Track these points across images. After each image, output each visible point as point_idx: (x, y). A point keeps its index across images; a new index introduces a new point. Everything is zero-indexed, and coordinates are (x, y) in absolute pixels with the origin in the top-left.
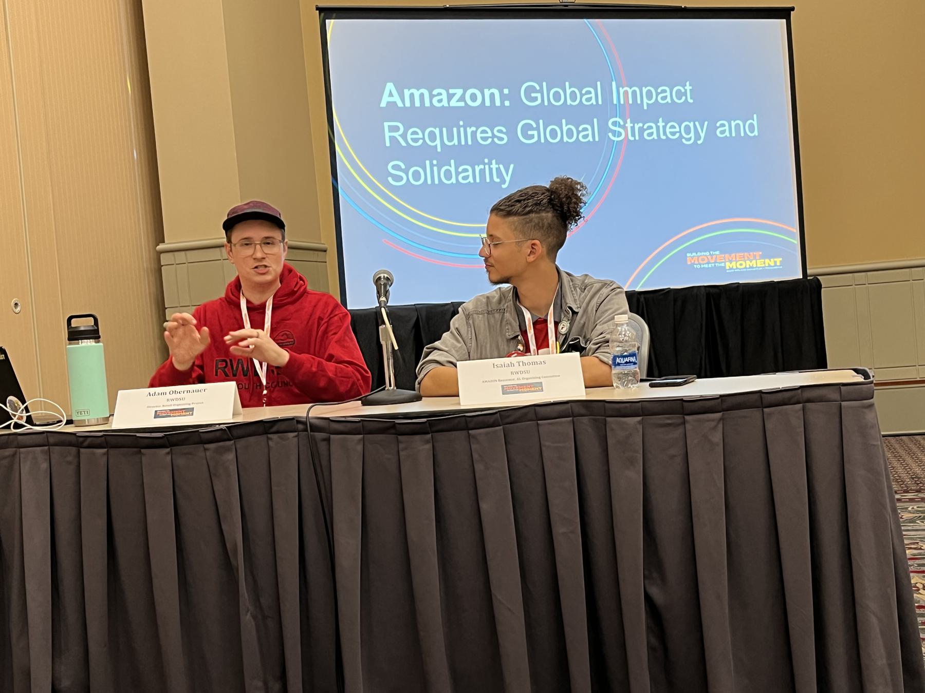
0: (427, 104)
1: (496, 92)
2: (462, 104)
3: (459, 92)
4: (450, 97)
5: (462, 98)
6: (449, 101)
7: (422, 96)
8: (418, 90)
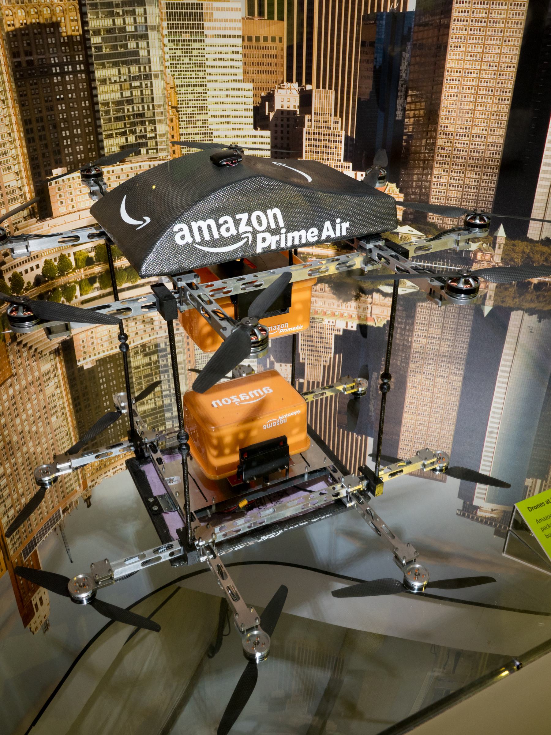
0: (216, 236)
1: (277, 211)
2: (250, 229)
3: (244, 217)
4: (237, 223)
5: (249, 223)
6: (237, 227)
7: (209, 227)
8: (205, 221)
